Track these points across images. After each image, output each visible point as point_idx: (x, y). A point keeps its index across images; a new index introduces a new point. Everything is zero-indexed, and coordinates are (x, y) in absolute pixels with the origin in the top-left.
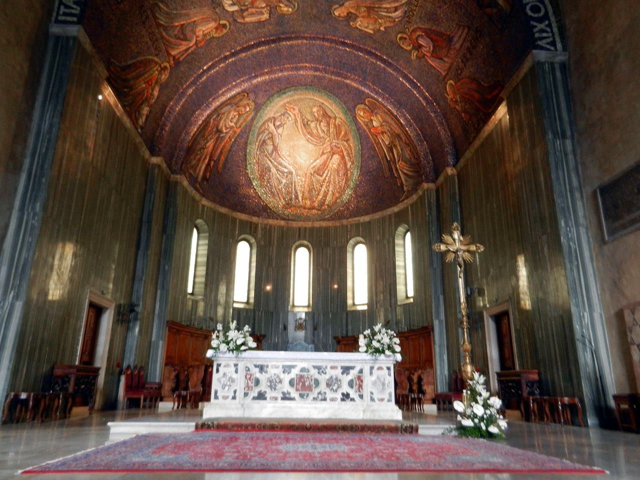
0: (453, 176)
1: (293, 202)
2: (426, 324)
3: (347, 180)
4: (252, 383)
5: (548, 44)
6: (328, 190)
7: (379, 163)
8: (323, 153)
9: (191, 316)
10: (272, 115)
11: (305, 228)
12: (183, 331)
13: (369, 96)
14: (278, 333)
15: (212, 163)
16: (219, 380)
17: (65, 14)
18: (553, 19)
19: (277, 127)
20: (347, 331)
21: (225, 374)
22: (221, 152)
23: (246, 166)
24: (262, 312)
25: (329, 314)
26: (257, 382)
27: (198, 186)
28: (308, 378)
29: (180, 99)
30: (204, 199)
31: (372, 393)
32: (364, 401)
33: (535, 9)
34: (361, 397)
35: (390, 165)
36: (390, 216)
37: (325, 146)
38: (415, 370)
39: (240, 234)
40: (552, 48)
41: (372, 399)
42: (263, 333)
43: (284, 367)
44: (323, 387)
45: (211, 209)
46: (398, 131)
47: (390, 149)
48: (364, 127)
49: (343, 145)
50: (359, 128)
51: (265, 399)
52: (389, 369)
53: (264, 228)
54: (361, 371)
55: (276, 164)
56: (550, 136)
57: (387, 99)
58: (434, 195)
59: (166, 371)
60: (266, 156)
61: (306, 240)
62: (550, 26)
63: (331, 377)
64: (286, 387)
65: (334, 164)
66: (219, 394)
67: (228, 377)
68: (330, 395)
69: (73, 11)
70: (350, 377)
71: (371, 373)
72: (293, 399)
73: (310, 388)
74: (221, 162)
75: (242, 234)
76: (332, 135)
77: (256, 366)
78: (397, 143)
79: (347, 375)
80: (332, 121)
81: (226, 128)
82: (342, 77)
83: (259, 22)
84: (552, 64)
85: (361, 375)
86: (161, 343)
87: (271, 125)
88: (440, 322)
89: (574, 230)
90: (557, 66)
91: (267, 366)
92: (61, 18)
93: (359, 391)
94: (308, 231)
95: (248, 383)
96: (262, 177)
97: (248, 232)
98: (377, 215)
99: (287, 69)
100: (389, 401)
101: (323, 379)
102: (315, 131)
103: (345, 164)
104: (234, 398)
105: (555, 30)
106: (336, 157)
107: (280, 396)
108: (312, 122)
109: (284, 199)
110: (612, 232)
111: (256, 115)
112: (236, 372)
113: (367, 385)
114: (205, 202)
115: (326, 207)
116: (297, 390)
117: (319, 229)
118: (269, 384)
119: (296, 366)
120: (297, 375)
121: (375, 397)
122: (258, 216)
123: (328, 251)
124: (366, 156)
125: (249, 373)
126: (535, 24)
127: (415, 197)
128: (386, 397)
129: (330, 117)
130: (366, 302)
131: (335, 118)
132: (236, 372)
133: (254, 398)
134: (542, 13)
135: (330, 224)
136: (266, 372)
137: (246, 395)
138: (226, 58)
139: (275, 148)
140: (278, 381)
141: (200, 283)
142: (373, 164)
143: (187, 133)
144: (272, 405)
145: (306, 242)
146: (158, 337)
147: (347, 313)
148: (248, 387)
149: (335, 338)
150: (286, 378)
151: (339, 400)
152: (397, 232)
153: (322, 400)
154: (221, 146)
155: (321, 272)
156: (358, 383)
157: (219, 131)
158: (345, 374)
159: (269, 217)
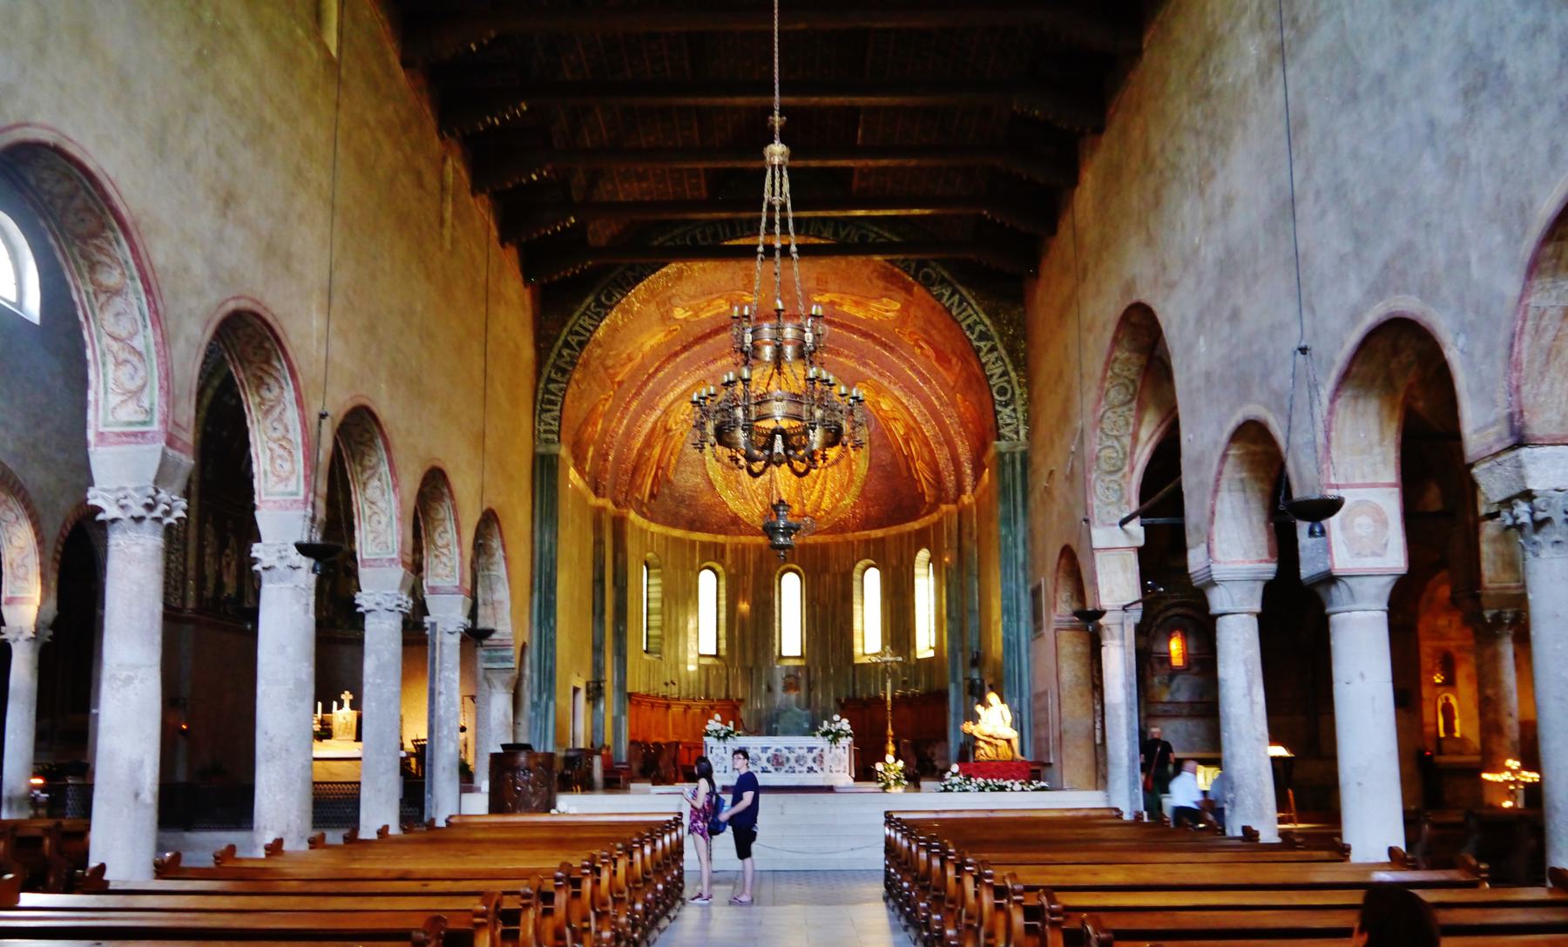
0: (970, 505)
3: (851, 474)
6: (825, 489)
7: (894, 456)
17: (546, 432)
18: (1019, 402)
22: (671, 454)
23: (705, 465)
27: (645, 510)
29: (623, 417)
30: (653, 524)
33: (1002, 391)
34: (822, 769)
35: (907, 463)
36: (909, 533)
39: (702, 561)
40: (1015, 437)
42: (740, 696)
44: (792, 763)
45: (662, 534)
46: (911, 423)
47: (907, 442)
48: (871, 407)
53: (735, 550)
54: (822, 750)
57: (895, 384)
58: (956, 516)
62: (1014, 410)
68: (798, 768)
69: (552, 428)
73: (782, 764)
74: (671, 467)
78: (913, 436)
81: (676, 423)
82: (834, 354)
83: (718, 314)
84: (1013, 454)
86: (623, 718)
88: (957, 685)
89: (1015, 625)
90: (1018, 456)
92: (543, 436)
97: (712, 557)
98: (893, 530)
101: (792, 756)
105: (1020, 415)
109: (761, 503)
114: (655, 528)
115: (823, 513)
117: (814, 547)
122: (726, 534)
123: (827, 578)
124: (876, 443)
127: (935, 517)
134: (1009, 395)
135: (828, 539)
138: (676, 354)
142: (885, 457)
143: (630, 449)
145: (795, 566)
147: (855, 666)
149: (838, 700)
150: (764, 757)
154: (670, 447)
155: (818, 609)
157: (667, 430)
159: (741, 533)
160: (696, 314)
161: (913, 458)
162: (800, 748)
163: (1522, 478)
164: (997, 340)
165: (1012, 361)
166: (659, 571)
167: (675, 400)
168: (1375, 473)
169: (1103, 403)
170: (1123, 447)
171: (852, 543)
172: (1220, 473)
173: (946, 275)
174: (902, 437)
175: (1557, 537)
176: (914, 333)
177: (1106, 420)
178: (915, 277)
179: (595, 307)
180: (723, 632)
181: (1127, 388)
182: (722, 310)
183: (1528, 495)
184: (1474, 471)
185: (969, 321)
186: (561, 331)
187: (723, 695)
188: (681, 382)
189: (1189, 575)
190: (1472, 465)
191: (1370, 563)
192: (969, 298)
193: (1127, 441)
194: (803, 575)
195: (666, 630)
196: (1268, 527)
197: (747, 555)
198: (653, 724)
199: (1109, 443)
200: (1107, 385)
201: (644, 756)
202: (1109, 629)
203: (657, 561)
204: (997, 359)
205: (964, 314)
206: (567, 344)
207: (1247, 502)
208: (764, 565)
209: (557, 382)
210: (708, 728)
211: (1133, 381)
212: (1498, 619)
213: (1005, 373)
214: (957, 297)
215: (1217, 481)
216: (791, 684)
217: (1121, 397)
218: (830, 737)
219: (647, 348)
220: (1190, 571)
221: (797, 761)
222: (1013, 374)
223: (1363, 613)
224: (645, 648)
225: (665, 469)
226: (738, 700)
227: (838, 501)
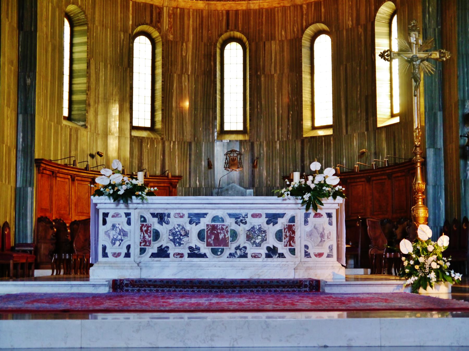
4: (150, 237)
9: (70, 152)
11: (237, 11)
12: (59, 172)
14: (200, 173)
16: (107, 233)
21: (114, 226)
24: (174, 142)
25: (276, 142)
26: (157, 235)
28: (222, 229)
31: (306, 247)
32: (296, 257)
34: (293, 251)
39: (136, 25)
41: (307, 255)
42: (177, 174)
43: (190, 215)
44: (242, 241)
51: (168, 256)
52: (329, 215)
54: (292, 219)
59: (41, 228)
61: (238, 31)
63: (253, 228)
64: (194, 241)
67: (118, 230)
68: (251, 250)
70: (278, 227)
71: (306, 222)
72: (204, 256)
73: (225, 243)
75: (140, 25)
77: (153, 215)
79: (273, 225)
85: (292, 224)
86: (29, 189)
91: (169, 216)
93: (290, 245)
94: (240, 17)
95: (144, 237)
97: (148, 21)
100: (329, 256)
101: (242, 230)
104: (128, 255)
107: (186, 252)
112: (129, 223)
113: (300, 237)
116: (208, 244)
118: (171, 237)
119: (206, 214)
120: (207, 225)
121: (310, 251)
123: (273, 46)
125: (145, 224)
128: (326, 251)
130: (330, 122)
132: (129, 223)
133: (153, 255)
136: (168, 223)
137: (142, 251)
140: (183, 233)
144: (176, 264)
147: (303, 141)
148: (144, 241)
150: (194, 230)
151: (264, 256)
152: (377, 14)
153: (241, 256)
156: (288, 234)
158: (272, 224)
162: (254, 216)
166: (85, 28)
171: (301, 6)
180: (158, 103)
187: (158, 172)
195: (92, 95)
197: (186, 22)
198: (74, 200)
201: (57, 235)
203: (82, 16)
208: (205, 33)
210: (101, 181)
216: (233, 160)
218: (307, 197)
221: (249, 238)
224: (66, 113)
226: (174, 177)
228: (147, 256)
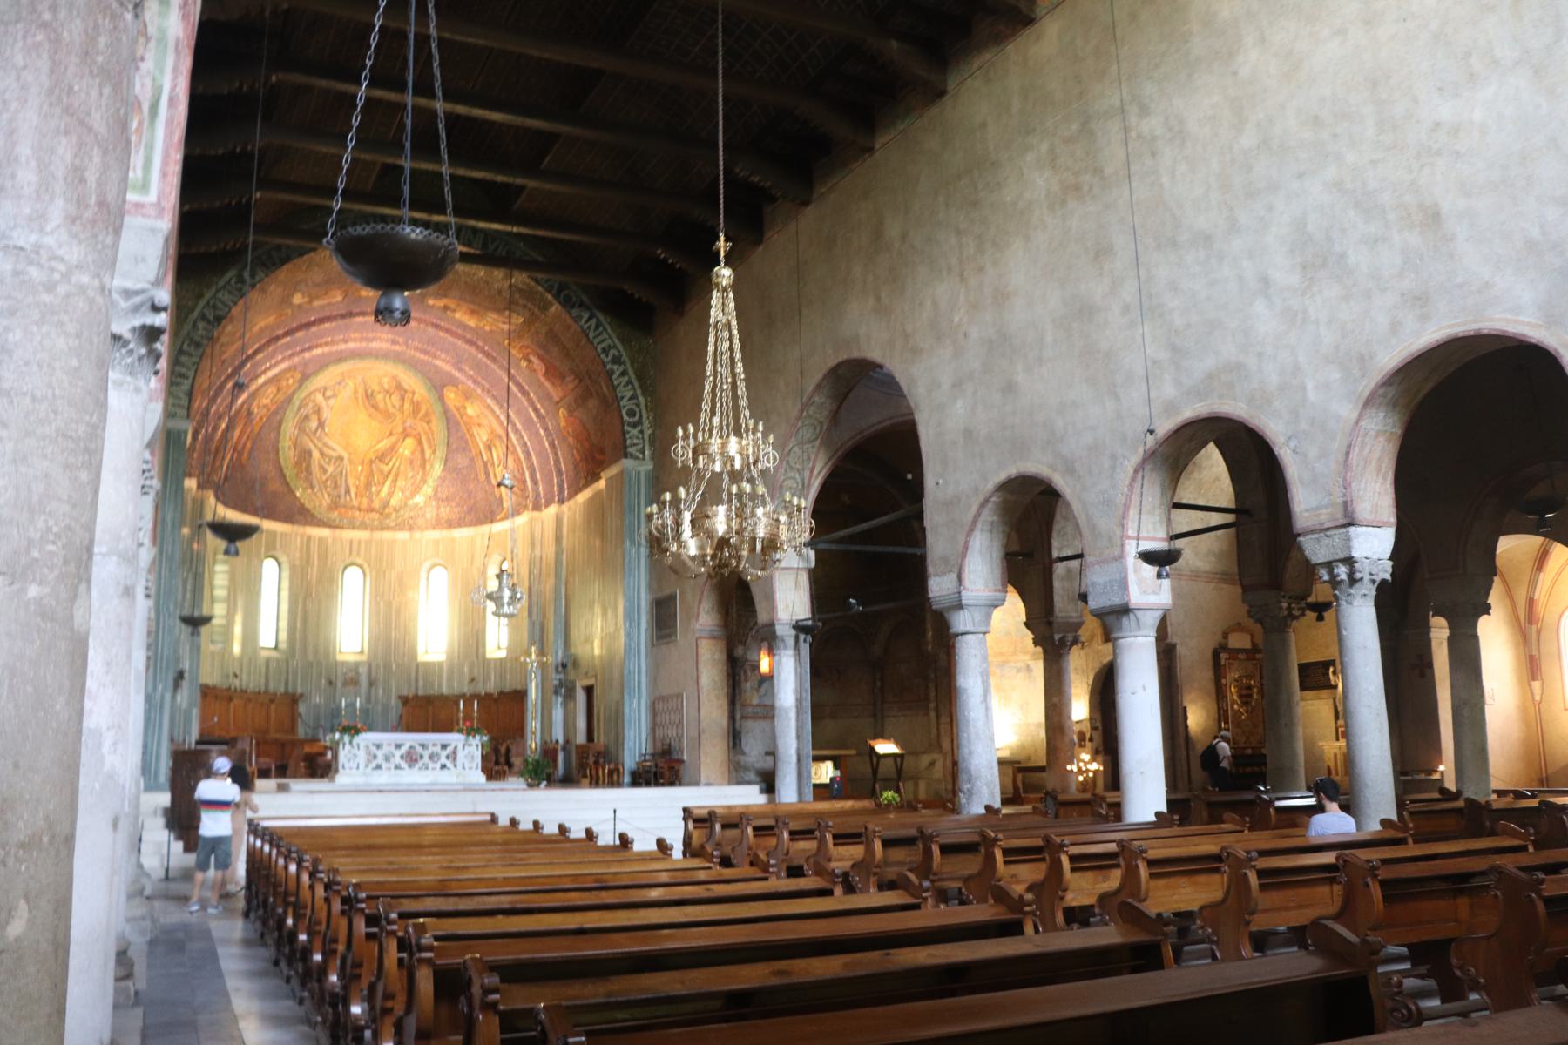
1: (342, 500)
2: (519, 688)
5: (637, 451)
7: (472, 460)
8: (391, 434)
10: (323, 384)
13: (463, 383)
15: (235, 455)
19: (329, 398)
20: (417, 689)
33: (631, 413)
34: (455, 766)
37: (394, 424)
38: (504, 741)
40: (641, 456)
41: (464, 768)
42: (299, 691)
44: (426, 759)
47: (489, 448)
49: (421, 427)
50: (446, 411)
54: (456, 748)
55: (320, 445)
56: (628, 543)
60: (307, 435)
62: (642, 432)
64: (397, 760)
65: (405, 449)
66: (346, 766)
68: (431, 765)
69: (182, 402)
73: (416, 761)
74: (246, 451)
76: (406, 413)
80: (408, 397)
87: (319, 398)
96: (298, 464)
99: (355, 340)
101: (426, 754)
102: (381, 405)
103: (423, 452)
104: (358, 768)
105: (646, 437)
106: (410, 442)
107: (393, 767)
108: (379, 392)
109: (329, 495)
110: (658, 638)
111: (300, 386)
124: (454, 446)
126: (629, 429)
128: (474, 766)
129: (406, 391)
131: (414, 393)
137: (367, 766)
139: (321, 425)
141: (220, 626)
146: (190, 705)
148: (369, 761)
149: (400, 697)
150: (398, 753)
157: (250, 413)
160: (310, 302)
161: (493, 464)
163: (1349, 548)
164: (628, 365)
165: (641, 386)
167: (265, 383)
168: (1155, 530)
169: (793, 439)
170: (803, 480)
172: (978, 514)
173: (585, 299)
174: (484, 444)
175: (1364, 591)
176: (527, 347)
177: (792, 454)
178: (557, 297)
179: (236, 283)
181: (815, 429)
182: (335, 300)
183: (1349, 561)
184: (1301, 539)
185: (603, 345)
186: (197, 304)
188: (275, 365)
189: (929, 599)
190: (1299, 535)
191: (1152, 600)
192: (604, 323)
193: (807, 474)
194: (367, 571)
196: (1002, 563)
199: (792, 474)
200: (800, 424)
202: (783, 640)
204: (629, 382)
205: (601, 338)
206: (203, 317)
207: (991, 540)
209: (190, 355)
211: (821, 423)
212: (1062, 640)
213: (634, 397)
214: (594, 321)
215: (975, 521)
217: (808, 436)
219: (256, 329)
220: (931, 595)
222: (641, 399)
223: (1144, 639)
225: (240, 454)
227: (407, 499)
228: (369, 769)
